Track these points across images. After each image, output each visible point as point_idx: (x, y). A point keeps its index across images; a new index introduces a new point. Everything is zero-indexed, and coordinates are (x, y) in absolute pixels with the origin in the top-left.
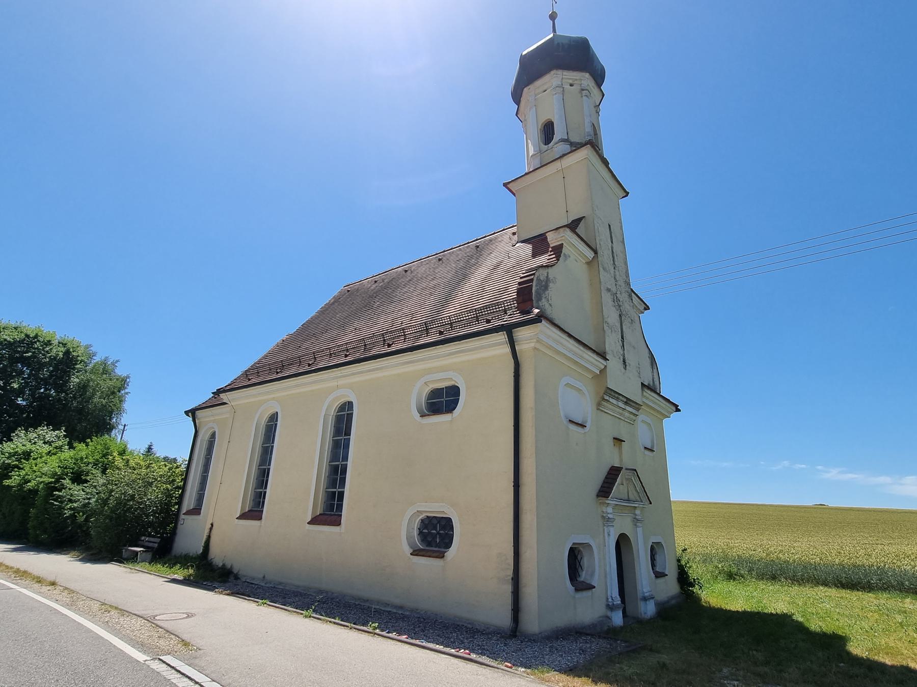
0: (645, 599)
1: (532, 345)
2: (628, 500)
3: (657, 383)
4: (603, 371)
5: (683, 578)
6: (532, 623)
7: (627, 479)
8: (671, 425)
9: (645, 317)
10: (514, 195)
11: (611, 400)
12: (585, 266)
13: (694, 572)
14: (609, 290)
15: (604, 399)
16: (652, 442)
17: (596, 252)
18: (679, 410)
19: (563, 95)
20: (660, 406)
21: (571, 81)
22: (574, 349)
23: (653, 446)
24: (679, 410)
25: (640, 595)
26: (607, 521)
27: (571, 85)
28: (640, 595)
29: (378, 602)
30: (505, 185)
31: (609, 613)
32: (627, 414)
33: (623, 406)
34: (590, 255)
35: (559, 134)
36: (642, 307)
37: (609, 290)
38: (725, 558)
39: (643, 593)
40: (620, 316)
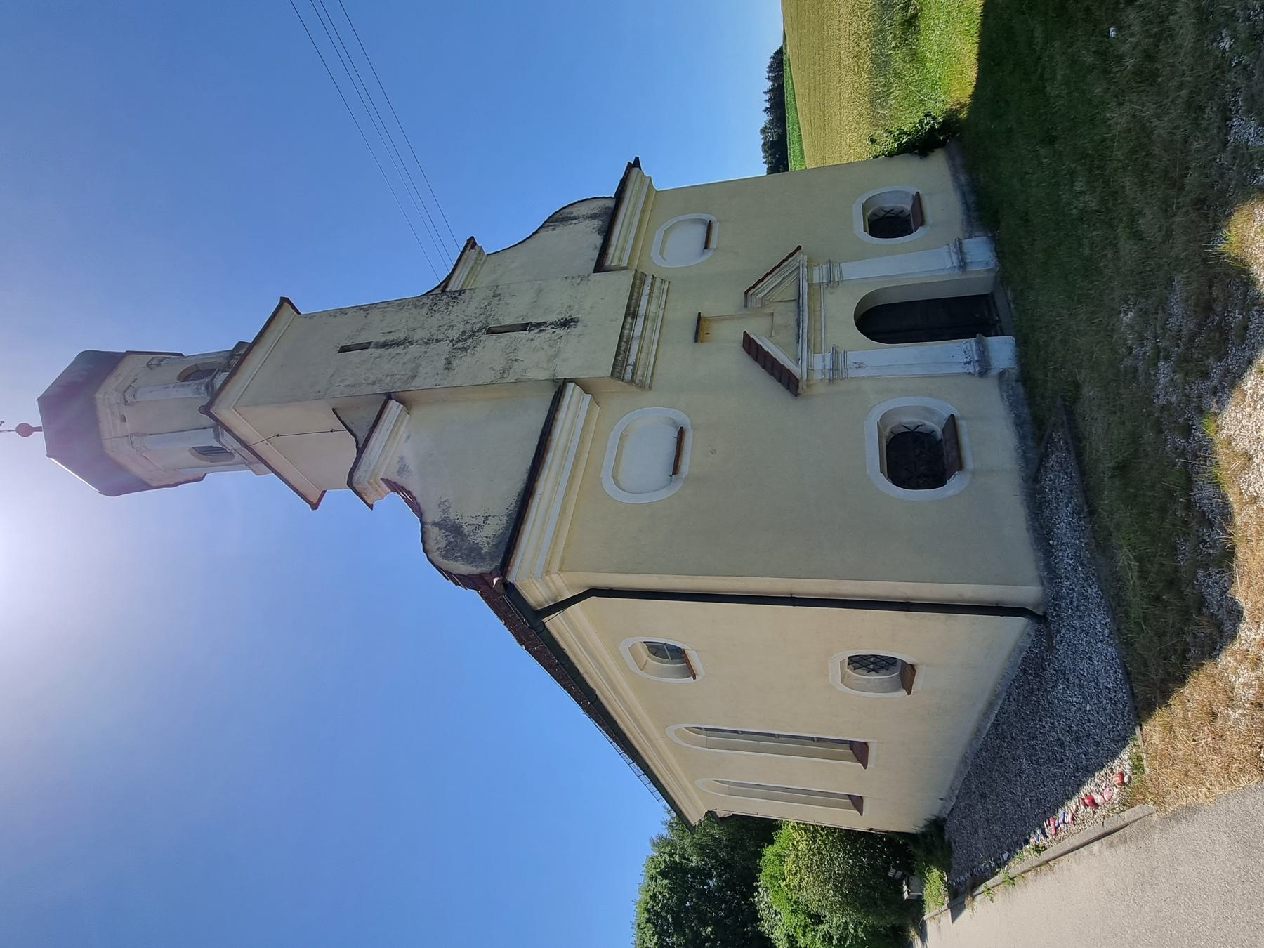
0: (963, 265)
1: (555, 576)
2: (798, 301)
3: (595, 207)
4: (585, 387)
5: (920, 145)
6: (1028, 592)
7: (763, 305)
8: (665, 175)
9: (488, 245)
10: (324, 492)
11: (632, 360)
12: (415, 412)
13: (910, 121)
14: (448, 365)
15: (632, 381)
16: (695, 221)
17: (389, 396)
18: (637, 159)
19: (143, 435)
20: (632, 217)
21: (118, 421)
22: (553, 474)
23: (703, 221)
24: (637, 159)
25: (957, 275)
26: (836, 372)
27: (124, 419)
28: (957, 275)
29: (985, 715)
30: (315, 506)
31: (994, 372)
32: (653, 308)
33: (640, 321)
34: (394, 405)
35: (207, 439)
36: (472, 254)
37: (448, 365)
38: (878, 36)
39: (953, 268)
40: (491, 332)
